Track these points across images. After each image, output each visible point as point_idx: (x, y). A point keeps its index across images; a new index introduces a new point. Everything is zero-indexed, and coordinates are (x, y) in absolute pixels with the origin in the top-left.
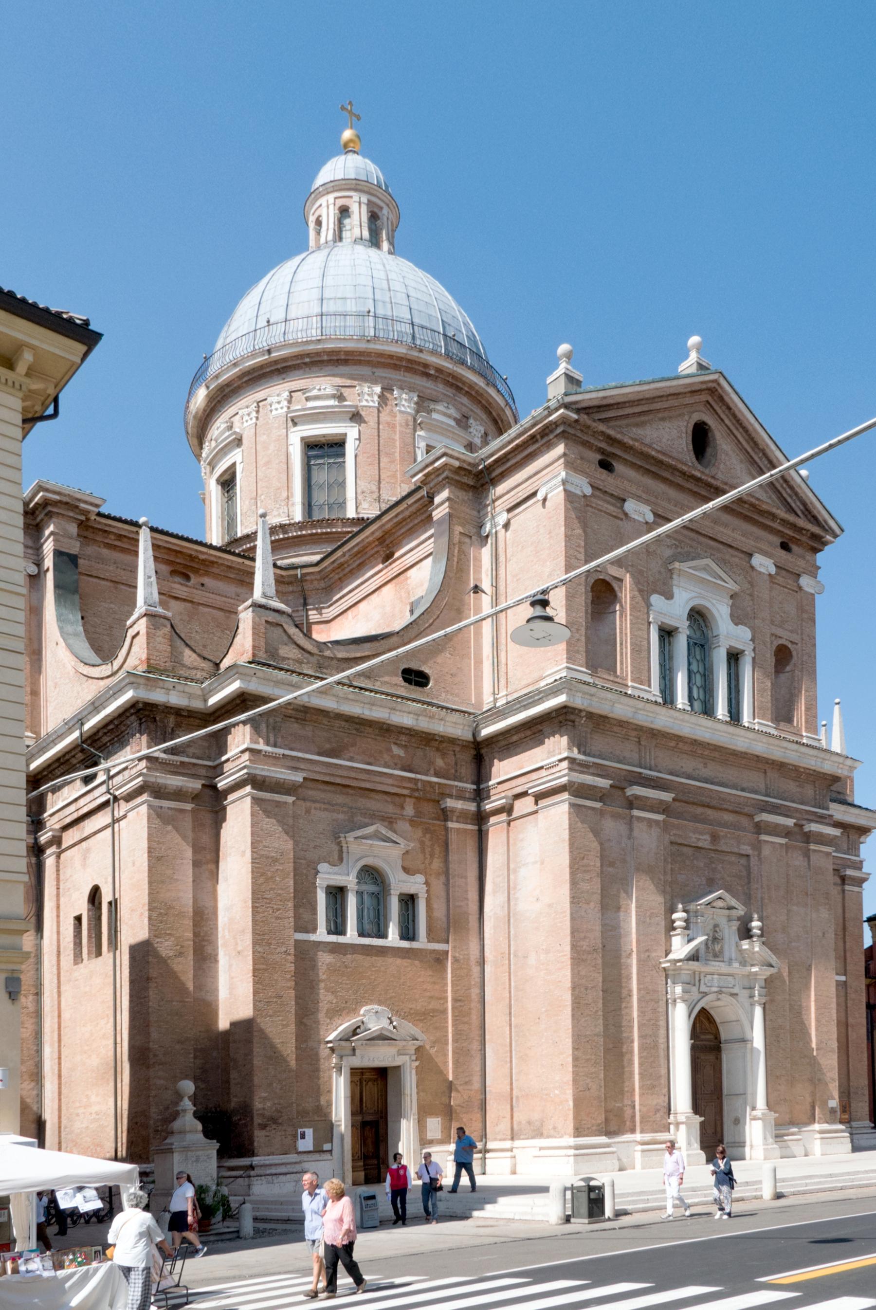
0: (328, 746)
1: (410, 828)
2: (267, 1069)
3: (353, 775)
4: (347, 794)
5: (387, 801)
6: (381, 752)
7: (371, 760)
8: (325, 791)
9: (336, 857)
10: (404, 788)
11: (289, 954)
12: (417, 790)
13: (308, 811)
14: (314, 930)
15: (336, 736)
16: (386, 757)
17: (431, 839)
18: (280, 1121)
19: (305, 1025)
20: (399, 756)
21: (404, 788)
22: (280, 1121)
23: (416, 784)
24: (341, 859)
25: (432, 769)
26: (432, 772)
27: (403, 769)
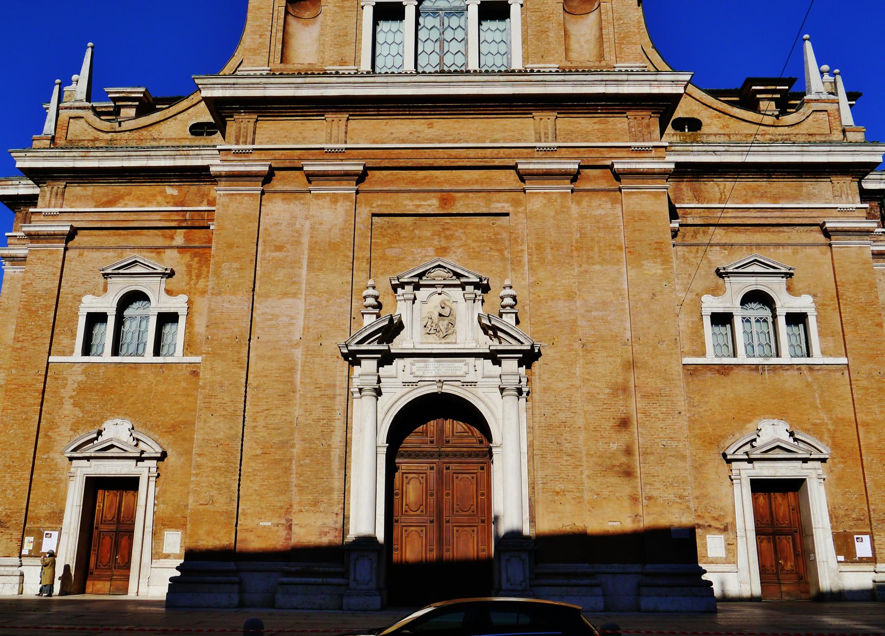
0: (105, 199)
1: (178, 255)
2: (4, 477)
3: (122, 217)
4: (120, 235)
5: (157, 235)
6: (154, 195)
7: (141, 204)
8: (99, 236)
9: (101, 288)
10: (172, 221)
11: (40, 375)
12: (186, 220)
13: (81, 255)
14: (71, 353)
15: (113, 190)
16: (159, 198)
17: (199, 262)
18: (8, 525)
19: (50, 437)
20: (172, 195)
21: (172, 221)
22: (8, 525)
23: (184, 216)
24: (105, 290)
25: (206, 201)
26: (205, 202)
27: (176, 205)
